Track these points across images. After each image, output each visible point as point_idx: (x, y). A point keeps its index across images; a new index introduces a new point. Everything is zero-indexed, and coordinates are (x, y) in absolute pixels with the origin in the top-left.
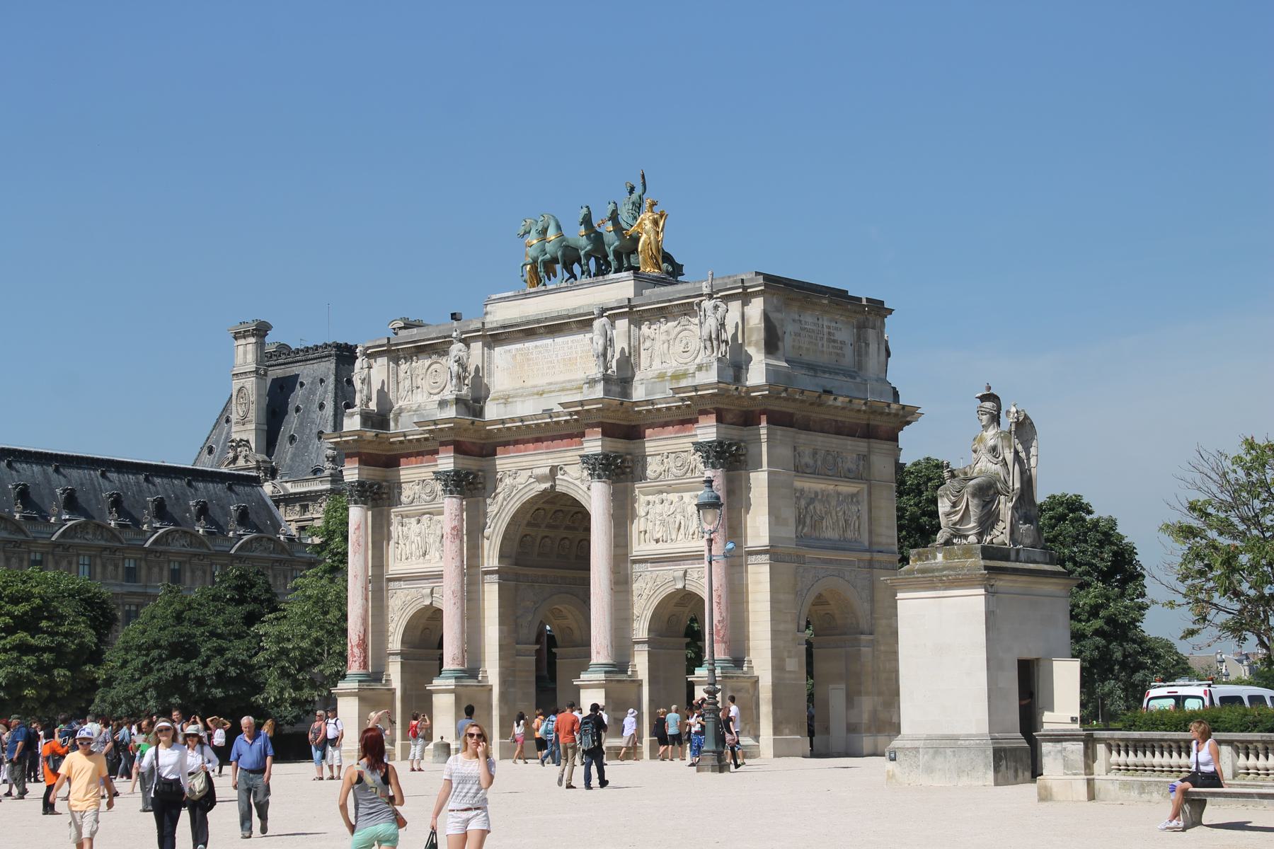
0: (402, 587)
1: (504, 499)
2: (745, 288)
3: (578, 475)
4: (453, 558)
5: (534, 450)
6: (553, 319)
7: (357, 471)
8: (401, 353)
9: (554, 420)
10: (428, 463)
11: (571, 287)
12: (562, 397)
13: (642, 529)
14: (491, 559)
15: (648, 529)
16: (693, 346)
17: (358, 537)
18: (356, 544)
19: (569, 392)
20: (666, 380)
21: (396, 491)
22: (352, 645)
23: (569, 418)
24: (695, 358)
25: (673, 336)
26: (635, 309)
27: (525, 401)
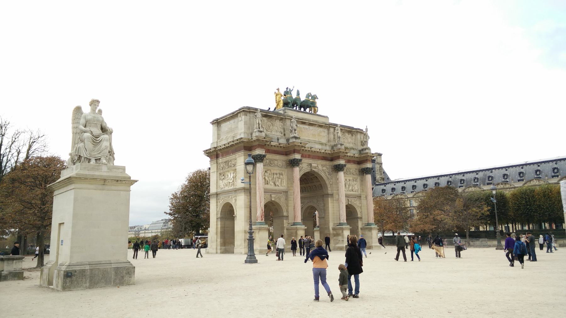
5: (308, 158)
6: (313, 122)
7: (264, 152)
9: (320, 151)
22: (263, 212)
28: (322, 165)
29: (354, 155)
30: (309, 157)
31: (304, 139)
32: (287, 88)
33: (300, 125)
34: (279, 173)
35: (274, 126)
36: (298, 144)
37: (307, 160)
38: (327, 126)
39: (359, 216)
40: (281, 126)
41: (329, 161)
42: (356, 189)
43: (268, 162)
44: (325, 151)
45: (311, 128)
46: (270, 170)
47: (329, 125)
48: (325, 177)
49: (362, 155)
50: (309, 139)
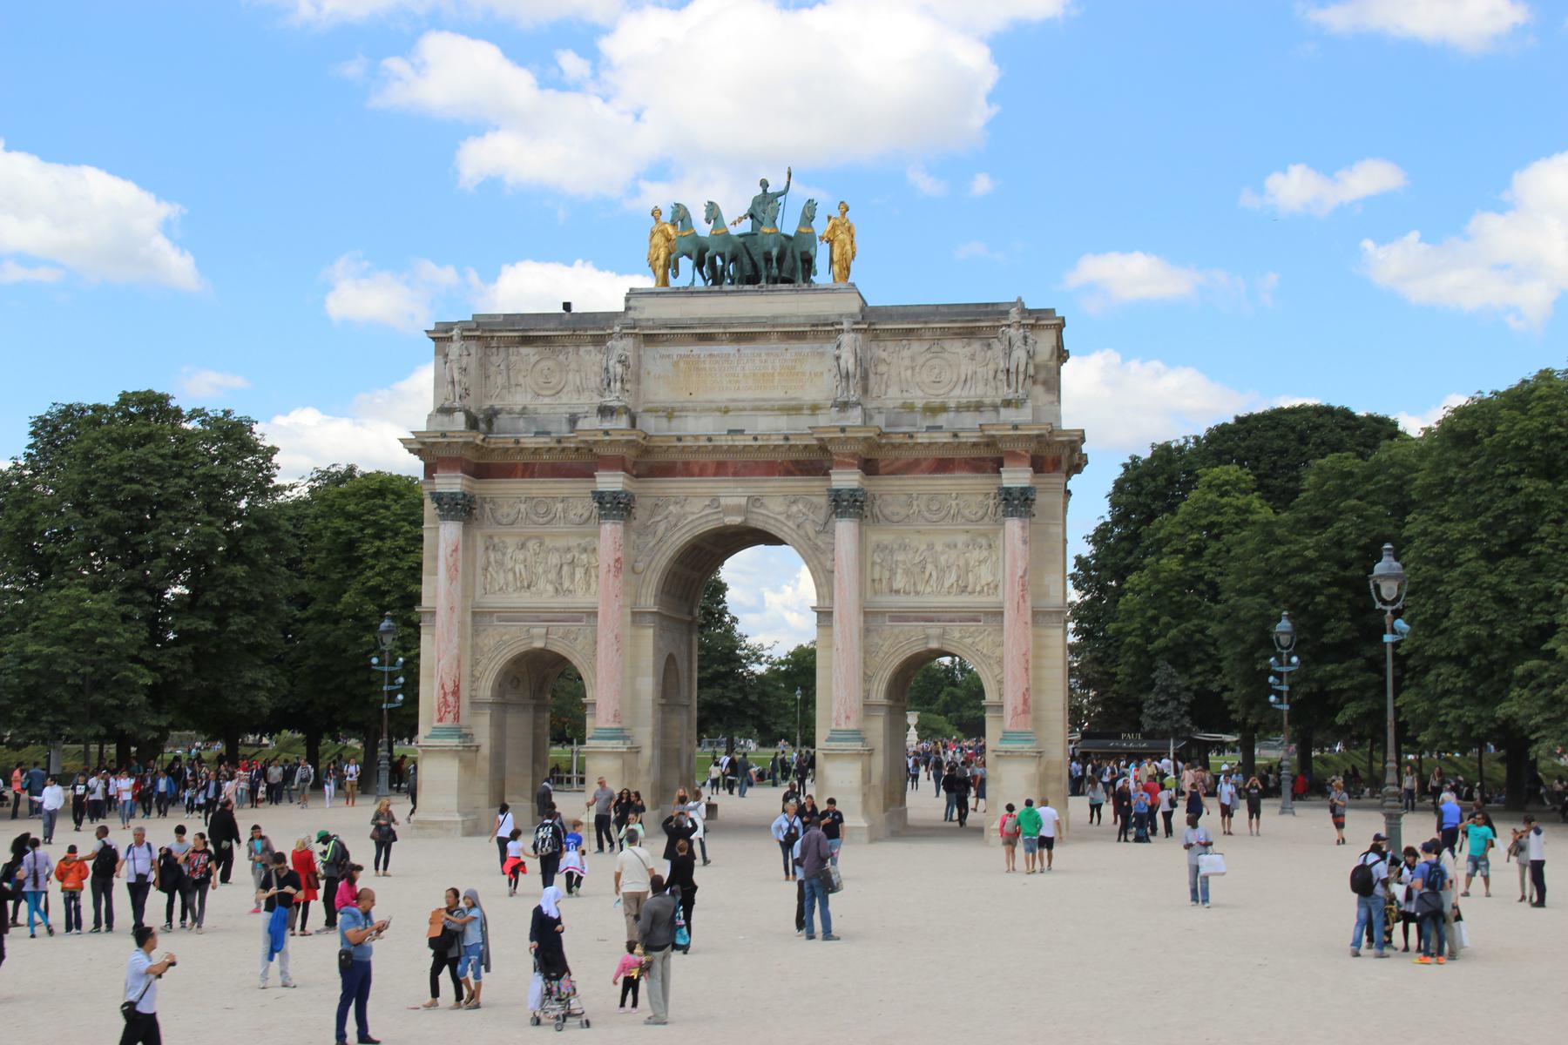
0: (495, 623)
1: (666, 529)
2: (1038, 319)
3: (781, 509)
5: (716, 474)
8: (494, 343)
9: (760, 443)
13: (877, 576)
14: (643, 599)
17: (456, 561)
21: (487, 507)
22: (445, 694)
23: (781, 443)
24: (951, 390)
25: (920, 361)
26: (873, 327)
29: (955, 435)
30: (720, 469)
31: (711, 402)
32: (764, 184)
33: (690, 348)
34: (579, 545)
35: (567, 373)
37: (710, 485)
39: (990, 696)
40: (596, 369)
42: (984, 583)
43: (523, 510)
45: (747, 349)
46: (537, 537)
47: (832, 325)
50: (735, 396)
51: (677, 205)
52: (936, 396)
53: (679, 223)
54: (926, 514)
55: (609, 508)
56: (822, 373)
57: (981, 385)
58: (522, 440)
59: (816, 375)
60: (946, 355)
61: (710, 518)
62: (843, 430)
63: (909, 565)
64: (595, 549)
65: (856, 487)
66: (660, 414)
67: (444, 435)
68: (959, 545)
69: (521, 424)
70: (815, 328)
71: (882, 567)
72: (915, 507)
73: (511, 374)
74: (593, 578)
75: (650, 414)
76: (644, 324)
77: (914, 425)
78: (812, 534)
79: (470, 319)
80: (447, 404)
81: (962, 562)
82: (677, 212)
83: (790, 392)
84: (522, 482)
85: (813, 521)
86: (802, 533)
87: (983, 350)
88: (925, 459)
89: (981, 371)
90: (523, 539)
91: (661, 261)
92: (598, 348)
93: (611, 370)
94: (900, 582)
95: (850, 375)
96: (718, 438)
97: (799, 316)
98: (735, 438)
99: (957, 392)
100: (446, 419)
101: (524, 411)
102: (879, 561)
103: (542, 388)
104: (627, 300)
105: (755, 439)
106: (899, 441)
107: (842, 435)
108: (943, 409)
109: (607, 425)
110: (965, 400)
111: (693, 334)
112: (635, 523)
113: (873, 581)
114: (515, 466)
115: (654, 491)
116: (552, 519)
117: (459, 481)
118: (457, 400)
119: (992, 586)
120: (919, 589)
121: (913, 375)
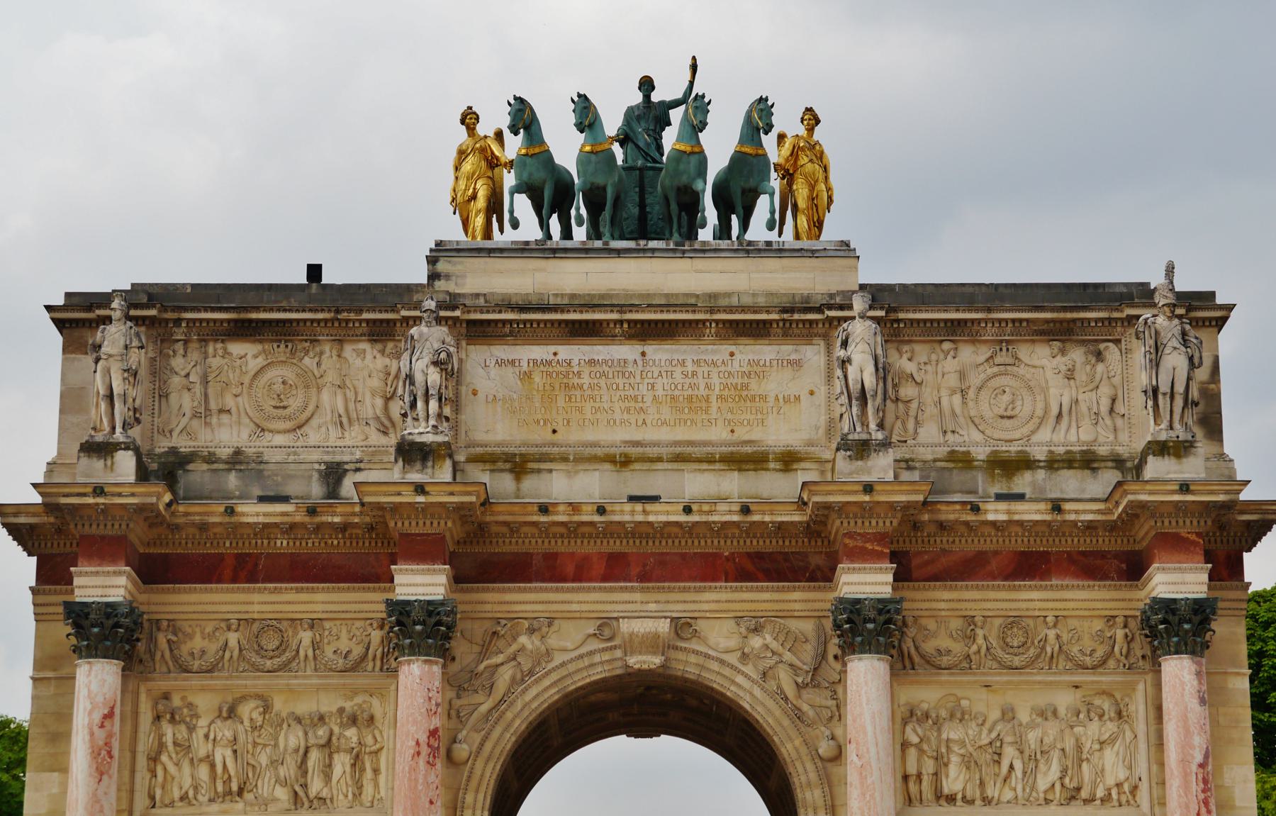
1: (513, 681)
3: (733, 643)
4: (431, 802)
5: (605, 579)
8: (179, 334)
9: (694, 518)
10: (270, 582)
11: (684, 252)
12: (686, 475)
13: (912, 769)
15: (924, 772)
16: (1027, 409)
17: (110, 736)
18: (103, 753)
19: (705, 466)
20: (976, 467)
21: (162, 639)
23: (736, 518)
24: (1033, 432)
25: (975, 380)
26: (893, 316)
27: (577, 472)
28: (738, 619)
29: (1057, 507)
31: (594, 445)
33: (552, 349)
34: (341, 711)
35: (319, 389)
36: (399, 494)
38: (811, 322)
40: (376, 383)
41: (812, 579)
42: (1110, 781)
44: (746, 510)
45: (659, 352)
46: (259, 697)
48: (770, 703)
49: (1117, 503)
50: (638, 437)
51: (520, 100)
52: (1010, 439)
53: (522, 131)
54: (1000, 653)
55: (420, 633)
56: (798, 398)
57: (1086, 423)
58: (239, 509)
59: (787, 400)
60: (1022, 370)
61: (597, 658)
62: (868, 488)
63: (971, 749)
64: (372, 718)
65: (888, 596)
66: (500, 465)
67: (99, 490)
68: (1062, 711)
69: (232, 480)
70: (786, 316)
71: (921, 752)
72: (980, 641)
73: (210, 391)
74: (369, 773)
75: (481, 466)
76: (468, 302)
77: (974, 492)
78: (790, 691)
79: (129, 288)
80: (99, 438)
81: (1069, 744)
82: (520, 110)
83: (735, 428)
84: (232, 591)
85: (791, 665)
86: (772, 685)
87: (1088, 362)
88: (996, 553)
89: (1086, 399)
90: (230, 699)
91: (481, 202)
92: (379, 346)
93: (419, 378)
94: (954, 781)
95: (868, 396)
96: (617, 508)
97: (754, 295)
98: (649, 507)
99: (1044, 435)
100: (98, 464)
101: (237, 459)
102: (915, 740)
103: (270, 418)
104: (432, 261)
105: (688, 510)
106: (952, 517)
107: (867, 498)
108: (1024, 463)
109: (415, 477)
110: (1061, 450)
111: (560, 322)
112: (454, 668)
113: (906, 778)
114: (220, 558)
115: (488, 607)
116: (290, 661)
117: (122, 580)
118: (119, 430)
119: (1126, 787)
120: (989, 793)
121: (964, 403)
